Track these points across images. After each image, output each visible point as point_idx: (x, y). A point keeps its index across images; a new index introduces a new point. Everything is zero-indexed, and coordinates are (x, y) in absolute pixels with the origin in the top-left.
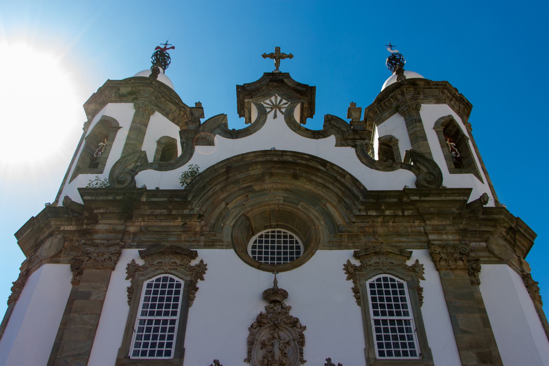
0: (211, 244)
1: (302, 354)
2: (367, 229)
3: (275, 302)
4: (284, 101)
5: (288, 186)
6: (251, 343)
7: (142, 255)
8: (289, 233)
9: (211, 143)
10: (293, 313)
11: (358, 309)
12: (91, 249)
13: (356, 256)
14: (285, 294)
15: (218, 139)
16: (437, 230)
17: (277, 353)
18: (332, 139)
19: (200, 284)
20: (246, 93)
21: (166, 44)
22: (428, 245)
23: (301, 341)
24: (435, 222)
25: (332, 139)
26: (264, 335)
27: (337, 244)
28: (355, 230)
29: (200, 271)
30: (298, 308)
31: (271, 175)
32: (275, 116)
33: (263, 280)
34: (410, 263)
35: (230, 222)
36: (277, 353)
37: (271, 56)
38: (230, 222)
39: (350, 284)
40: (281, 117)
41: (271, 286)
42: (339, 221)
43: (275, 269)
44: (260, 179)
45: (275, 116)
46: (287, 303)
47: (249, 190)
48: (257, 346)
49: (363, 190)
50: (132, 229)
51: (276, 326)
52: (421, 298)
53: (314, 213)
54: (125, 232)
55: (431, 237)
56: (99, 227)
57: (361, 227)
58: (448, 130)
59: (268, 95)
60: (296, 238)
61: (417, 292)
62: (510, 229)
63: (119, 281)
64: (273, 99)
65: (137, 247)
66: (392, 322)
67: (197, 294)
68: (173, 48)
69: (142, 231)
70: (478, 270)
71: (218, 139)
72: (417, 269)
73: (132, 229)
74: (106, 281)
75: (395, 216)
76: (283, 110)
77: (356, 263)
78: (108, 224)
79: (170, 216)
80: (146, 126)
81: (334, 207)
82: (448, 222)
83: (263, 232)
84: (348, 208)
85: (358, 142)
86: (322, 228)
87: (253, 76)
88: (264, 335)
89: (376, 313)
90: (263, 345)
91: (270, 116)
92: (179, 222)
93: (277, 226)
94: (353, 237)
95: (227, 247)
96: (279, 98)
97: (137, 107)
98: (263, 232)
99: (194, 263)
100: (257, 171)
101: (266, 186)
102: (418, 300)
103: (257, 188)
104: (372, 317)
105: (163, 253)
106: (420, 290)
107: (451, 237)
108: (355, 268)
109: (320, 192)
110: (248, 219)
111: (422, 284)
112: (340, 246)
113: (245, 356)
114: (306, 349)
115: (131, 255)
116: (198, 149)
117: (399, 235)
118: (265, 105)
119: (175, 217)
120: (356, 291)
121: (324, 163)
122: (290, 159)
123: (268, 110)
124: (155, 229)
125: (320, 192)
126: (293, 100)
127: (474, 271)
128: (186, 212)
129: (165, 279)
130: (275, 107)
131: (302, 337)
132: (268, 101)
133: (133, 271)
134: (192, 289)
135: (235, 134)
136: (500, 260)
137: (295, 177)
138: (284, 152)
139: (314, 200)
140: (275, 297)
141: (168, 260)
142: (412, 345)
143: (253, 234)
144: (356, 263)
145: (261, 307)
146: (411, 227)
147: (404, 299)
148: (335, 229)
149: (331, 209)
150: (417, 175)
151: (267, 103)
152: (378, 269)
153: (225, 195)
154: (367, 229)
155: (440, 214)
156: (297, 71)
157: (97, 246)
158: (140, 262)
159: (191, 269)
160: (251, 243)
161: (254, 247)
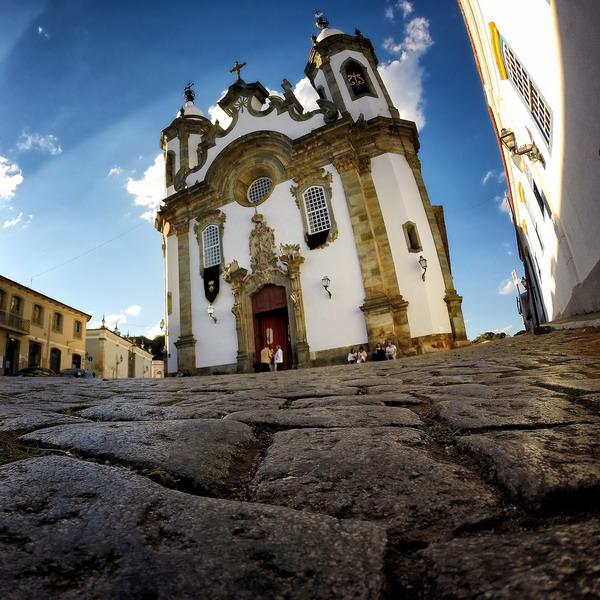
0: (225, 203)
3: (258, 222)
8: (266, 178)
9: (214, 145)
11: (298, 212)
14: (262, 216)
16: (337, 149)
18: (275, 111)
22: (331, 161)
24: (337, 143)
29: (223, 219)
31: (246, 150)
33: (250, 212)
34: (324, 175)
35: (231, 187)
39: (294, 199)
40: (245, 109)
44: (241, 155)
47: (238, 164)
48: (253, 246)
49: (290, 141)
51: (260, 235)
52: (331, 193)
53: (271, 164)
59: (236, 99)
61: (329, 190)
62: (391, 128)
63: (192, 235)
66: (317, 213)
67: (225, 230)
69: (195, 208)
70: (369, 163)
72: (328, 178)
73: (190, 209)
74: (187, 237)
75: (313, 148)
77: (296, 185)
79: (205, 196)
80: (187, 146)
81: (282, 156)
84: (288, 154)
86: (276, 172)
88: (255, 240)
89: (309, 211)
90: (256, 245)
92: (210, 197)
94: (292, 170)
99: (220, 215)
100: (238, 151)
102: (330, 195)
105: (205, 217)
106: (330, 189)
108: (295, 189)
109: (273, 149)
110: (240, 181)
111: (331, 185)
112: (287, 179)
115: (193, 222)
117: (317, 159)
120: (297, 202)
121: (268, 132)
122: (251, 138)
125: (273, 149)
126: (249, 95)
127: (364, 166)
130: (242, 104)
131: (273, 235)
133: (196, 229)
134: (222, 228)
135: (223, 133)
136: (384, 152)
137: (259, 146)
139: (271, 155)
140: (257, 219)
141: (208, 219)
142: (327, 222)
144: (296, 185)
145: (252, 227)
147: (322, 198)
148: (284, 169)
151: (236, 104)
152: (307, 185)
155: (339, 137)
156: (249, 78)
158: (198, 224)
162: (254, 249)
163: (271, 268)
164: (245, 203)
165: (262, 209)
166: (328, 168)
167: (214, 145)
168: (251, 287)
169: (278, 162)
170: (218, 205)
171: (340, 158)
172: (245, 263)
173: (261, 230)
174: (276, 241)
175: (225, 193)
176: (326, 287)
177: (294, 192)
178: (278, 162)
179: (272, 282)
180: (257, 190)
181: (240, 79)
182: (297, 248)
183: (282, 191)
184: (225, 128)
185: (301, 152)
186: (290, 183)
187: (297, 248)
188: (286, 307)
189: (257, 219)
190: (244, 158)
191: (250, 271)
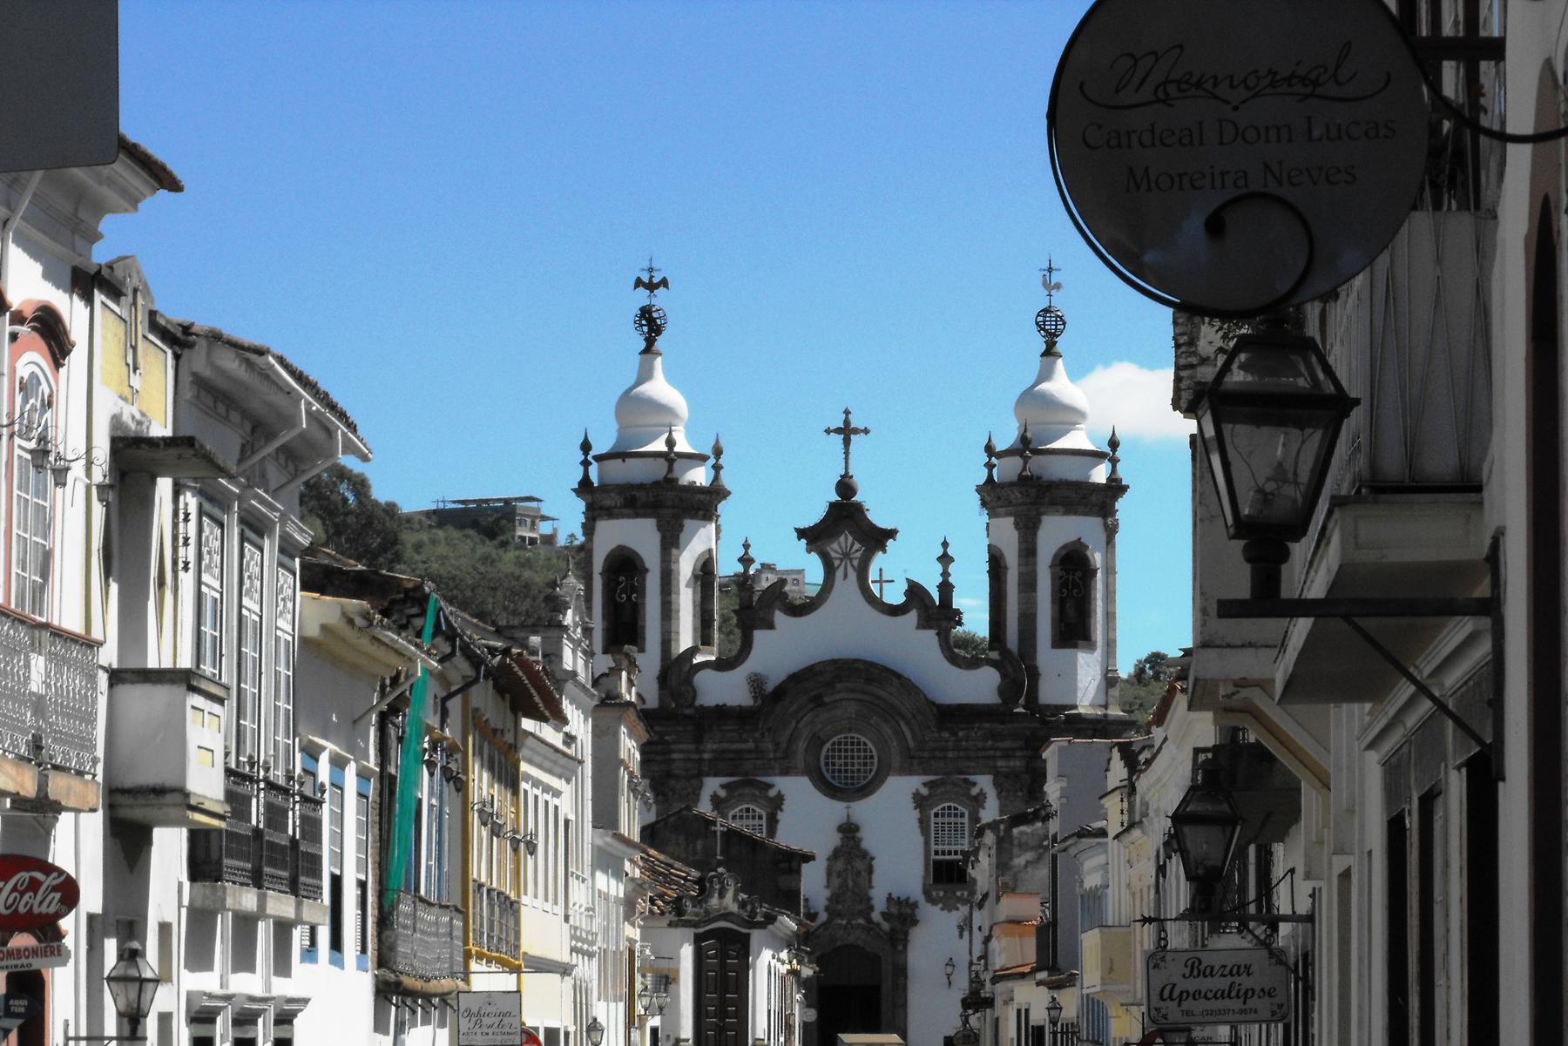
0: (786, 772)
1: (870, 881)
2: (937, 754)
4: (857, 546)
5: (860, 696)
6: (829, 874)
7: (723, 786)
8: (863, 739)
9: (771, 626)
10: (865, 845)
11: (921, 839)
12: (673, 782)
13: (925, 784)
15: (779, 617)
16: (1006, 757)
17: (850, 884)
18: (913, 616)
19: (780, 816)
21: (651, 270)
23: (870, 870)
24: (1007, 744)
25: (913, 616)
26: (840, 865)
27: (906, 770)
28: (926, 755)
29: (777, 803)
30: (870, 840)
32: (846, 576)
33: (835, 811)
34: (975, 791)
35: (801, 745)
36: (850, 884)
37: (838, 431)
38: (801, 745)
39: (916, 814)
40: (852, 575)
41: (844, 820)
42: (911, 744)
45: (846, 576)
46: (859, 835)
47: (818, 702)
50: (706, 756)
54: (701, 760)
55: (1000, 763)
56: (675, 756)
57: (934, 749)
60: (870, 745)
64: (842, 539)
65: (716, 775)
67: (779, 826)
68: (664, 283)
71: (779, 617)
76: (856, 563)
77: (924, 791)
78: (681, 751)
81: (908, 723)
82: (1020, 744)
83: (835, 739)
85: (945, 624)
87: (813, 515)
88: (840, 865)
90: (839, 876)
91: (839, 574)
93: (850, 730)
95: (803, 774)
96: (850, 539)
98: (835, 739)
101: (838, 697)
103: (826, 700)
104: (933, 847)
107: (1017, 764)
113: (824, 882)
114: (874, 876)
116: (759, 635)
117: (968, 758)
118: (833, 554)
119: (746, 741)
120: (921, 821)
121: (899, 676)
123: (837, 563)
124: (731, 756)
128: (757, 735)
129: (748, 810)
132: (835, 546)
135: (800, 609)
137: (869, 681)
138: (855, 661)
140: (849, 831)
141: (747, 790)
143: (824, 743)
144: (924, 791)
146: (984, 749)
149: (905, 728)
150: (1004, 676)
151: (834, 549)
153: (795, 707)
154: (937, 754)
157: (677, 777)
158: (722, 793)
159: (771, 800)
160: (824, 753)
161: (827, 757)
162: (836, 882)
163: (861, 921)
164: (832, 791)
165: (862, 810)
166: (984, 783)
167: (771, 626)
169: (899, 734)
170: (769, 771)
171: (1007, 776)
173: (851, 851)
174: (877, 878)
175: (788, 754)
176: (949, 976)
177: (920, 802)
178: (899, 734)
179: (860, 943)
181: (845, 487)
182: (915, 905)
183: (900, 789)
185: (946, 735)
187: (915, 905)
188: (877, 989)
189: (849, 831)
190: (838, 697)
191: (823, 917)
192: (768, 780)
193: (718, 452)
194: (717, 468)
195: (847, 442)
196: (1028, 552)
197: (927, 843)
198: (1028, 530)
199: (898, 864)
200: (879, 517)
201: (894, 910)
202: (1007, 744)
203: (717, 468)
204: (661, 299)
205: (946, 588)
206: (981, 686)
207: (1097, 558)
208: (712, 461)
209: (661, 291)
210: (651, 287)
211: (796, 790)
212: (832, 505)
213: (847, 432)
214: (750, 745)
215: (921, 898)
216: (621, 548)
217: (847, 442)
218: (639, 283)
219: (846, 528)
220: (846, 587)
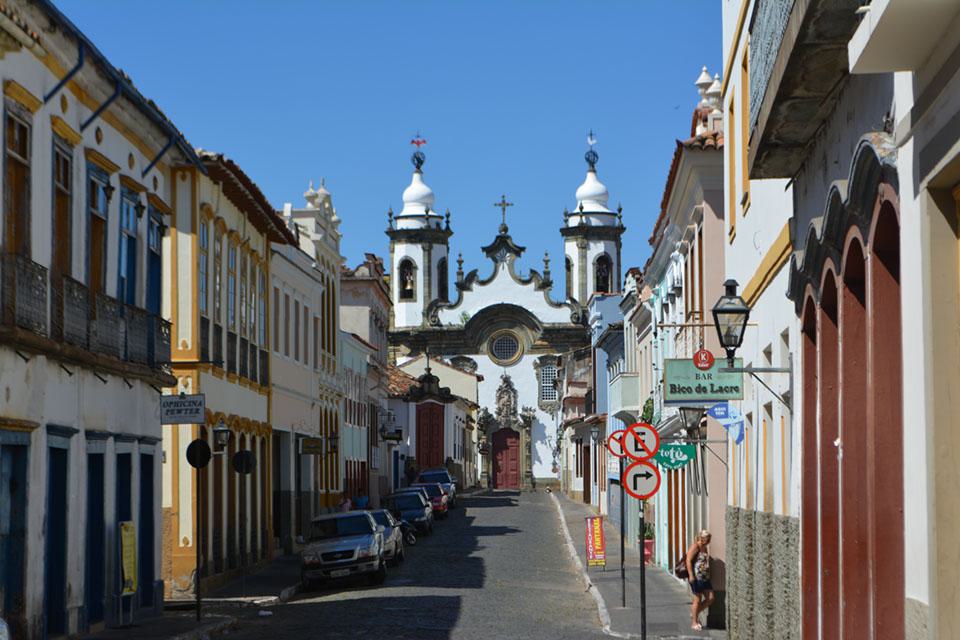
0: (477, 352)
11: (537, 382)
15: (475, 286)
18: (532, 285)
20: (490, 251)
24: (574, 340)
33: (501, 370)
39: (535, 371)
43: (505, 365)
58: (603, 262)
65: (448, 354)
82: (580, 339)
87: (489, 241)
92: (462, 341)
97: (423, 248)
103: (496, 320)
116: (466, 294)
135: (483, 283)
140: (507, 380)
144: (538, 361)
145: (500, 382)
150: (572, 310)
165: (510, 371)
168: (492, 429)
172: (492, 411)
173: (507, 387)
177: (536, 366)
180: (504, 351)
184: (482, 276)
186: (535, 357)
189: (507, 380)
192: (471, 357)
193: (448, 216)
194: (448, 222)
195: (504, 209)
196: (583, 257)
197: (539, 383)
198: (584, 248)
199: (528, 394)
200: (517, 240)
201: (526, 414)
202: (574, 340)
203: (448, 222)
204: (423, 148)
205: (547, 273)
206: (563, 317)
207: (614, 261)
208: (445, 219)
209: (422, 145)
210: (418, 143)
211: (483, 361)
212: (498, 237)
213: (504, 205)
214: (462, 341)
215: (537, 408)
216: (406, 257)
217: (504, 209)
218: (413, 142)
219: (501, 247)
220: (504, 272)
